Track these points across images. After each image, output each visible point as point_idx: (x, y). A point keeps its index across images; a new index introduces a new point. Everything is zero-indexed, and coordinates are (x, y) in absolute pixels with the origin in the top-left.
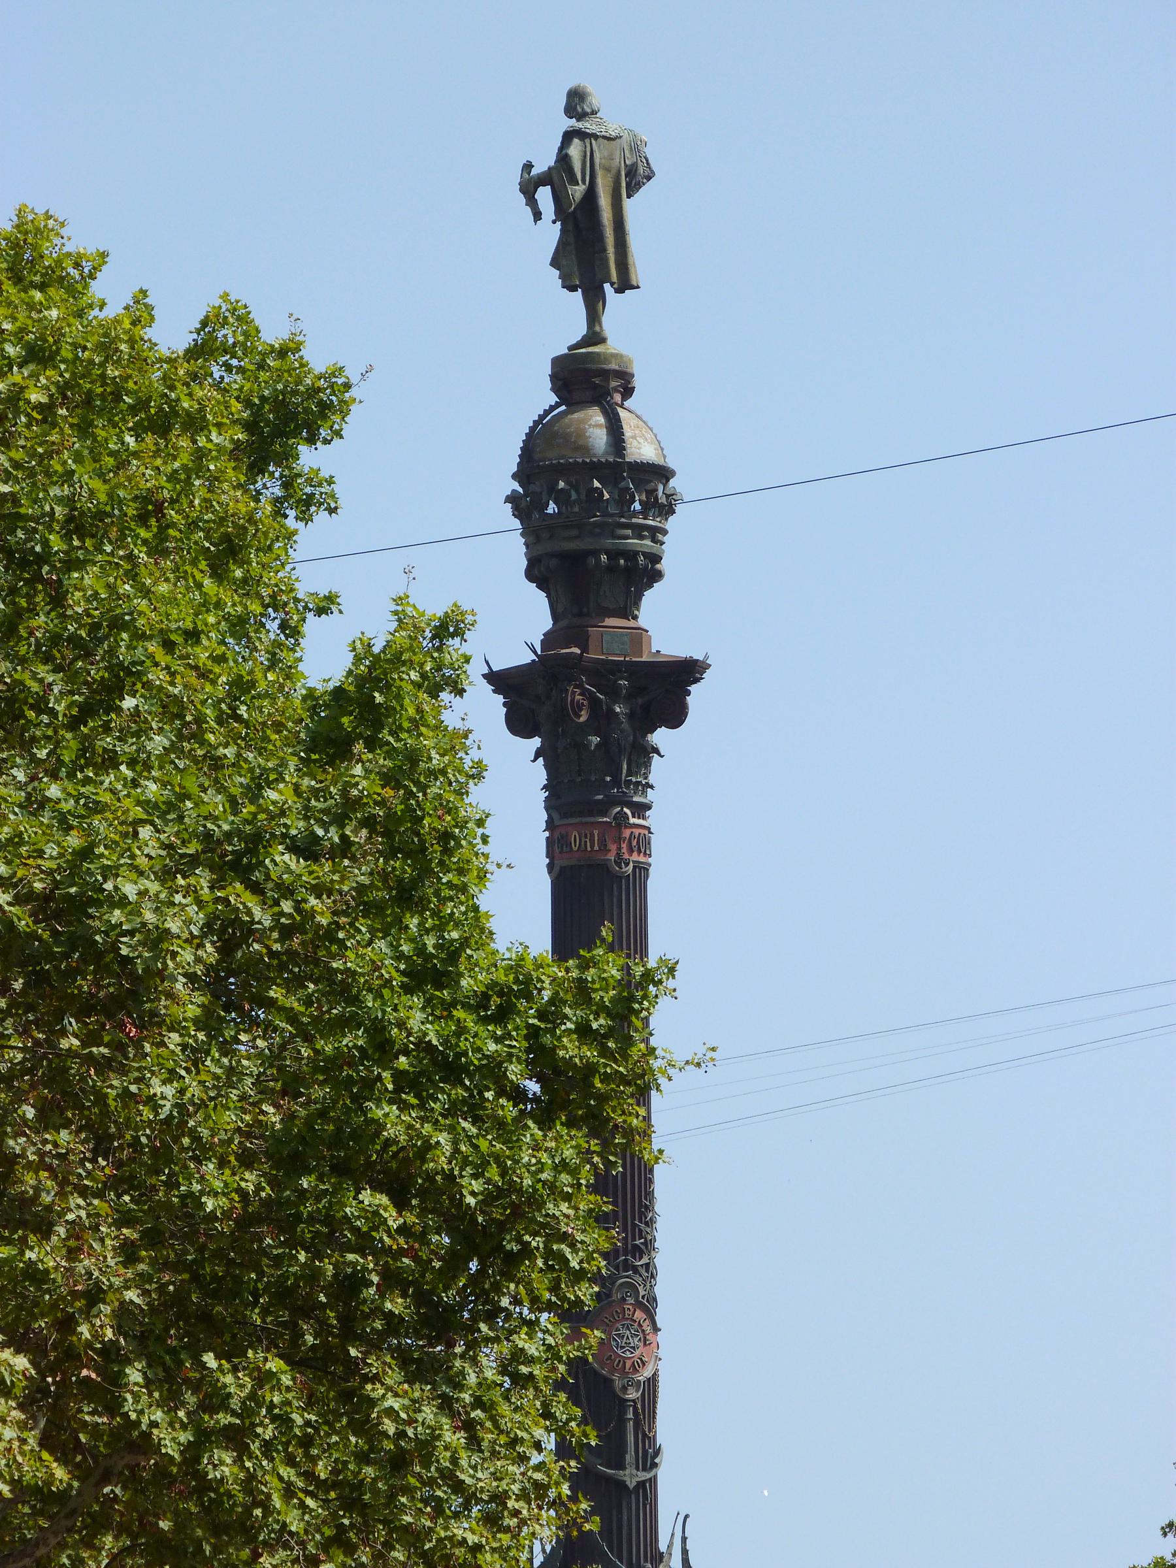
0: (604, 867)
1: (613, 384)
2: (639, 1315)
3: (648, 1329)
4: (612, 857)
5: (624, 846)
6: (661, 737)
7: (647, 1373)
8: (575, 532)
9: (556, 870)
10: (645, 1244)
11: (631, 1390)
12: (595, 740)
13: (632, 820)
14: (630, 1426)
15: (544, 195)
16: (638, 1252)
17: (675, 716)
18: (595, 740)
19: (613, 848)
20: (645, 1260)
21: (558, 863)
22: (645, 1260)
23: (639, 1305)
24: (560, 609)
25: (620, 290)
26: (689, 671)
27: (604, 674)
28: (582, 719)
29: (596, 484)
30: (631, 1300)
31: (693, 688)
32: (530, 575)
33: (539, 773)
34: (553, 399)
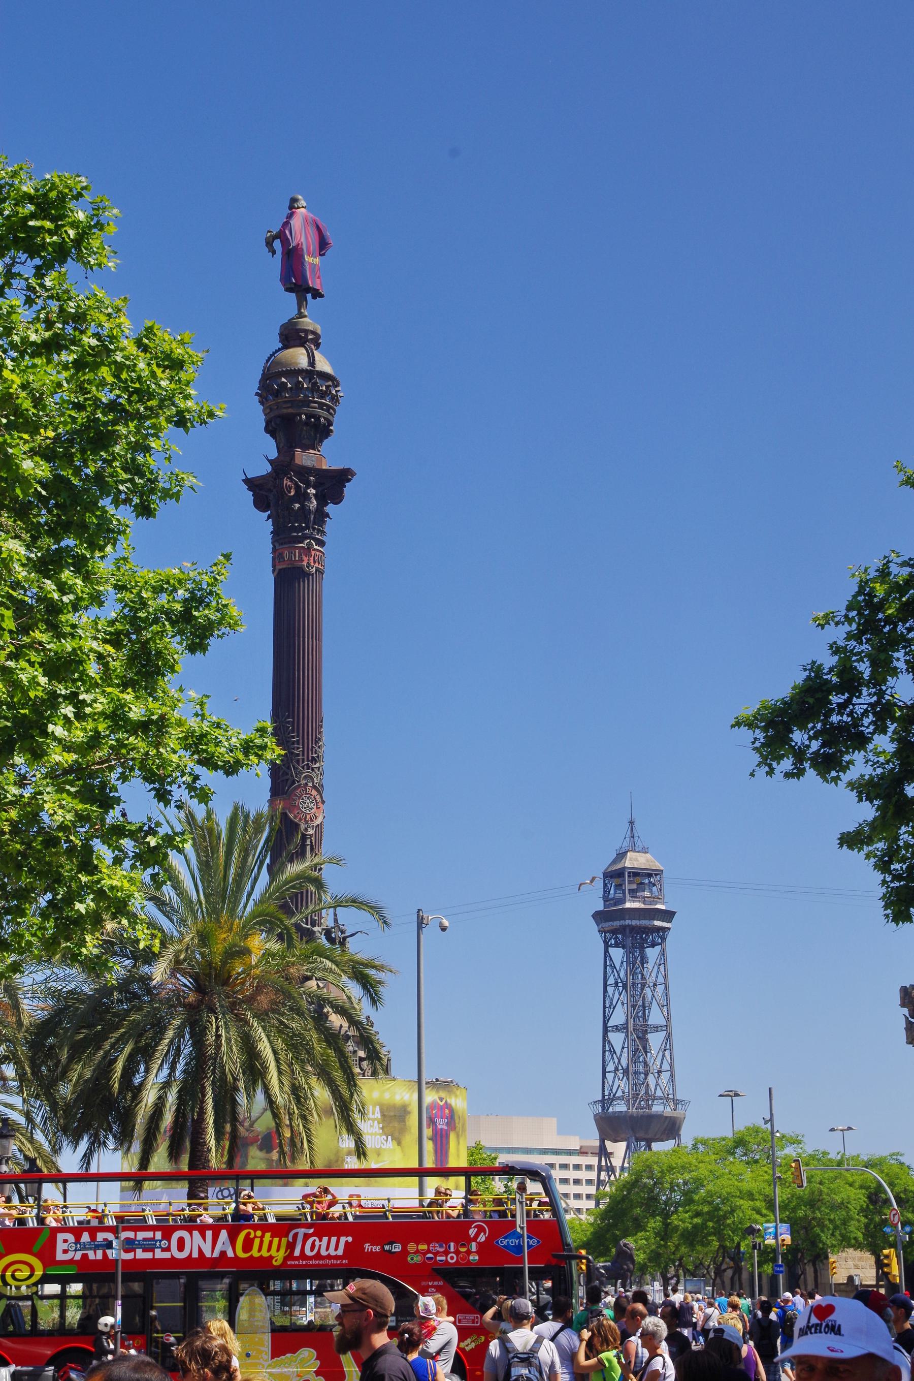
0: (301, 569)
1: (310, 337)
2: (314, 792)
3: (319, 800)
4: (305, 564)
5: (312, 559)
6: (330, 508)
7: (318, 822)
8: (289, 405)
9: (277, 571)
10: (318, 757)
11: (309, 830)
12: (297, 505)
13: (315, 547)
14: (308, 848)
15: (277, 244)
16: (314, 760)
17: (337, 498)
18: (297, 505)
19: (305, 559)
20: (317, 765)
21: (278, 567)
22: (317, 765)
23: (314, 787)
24: (282, 445)
25: (314, 297)
26: (343, 476)
27: (304, 472)
28: (292, 494)
29: (300, 379)
30: (310, 784)
31: (347, 484)
32: (267, 430)
33: (269, 526)
34: (280, 345)
